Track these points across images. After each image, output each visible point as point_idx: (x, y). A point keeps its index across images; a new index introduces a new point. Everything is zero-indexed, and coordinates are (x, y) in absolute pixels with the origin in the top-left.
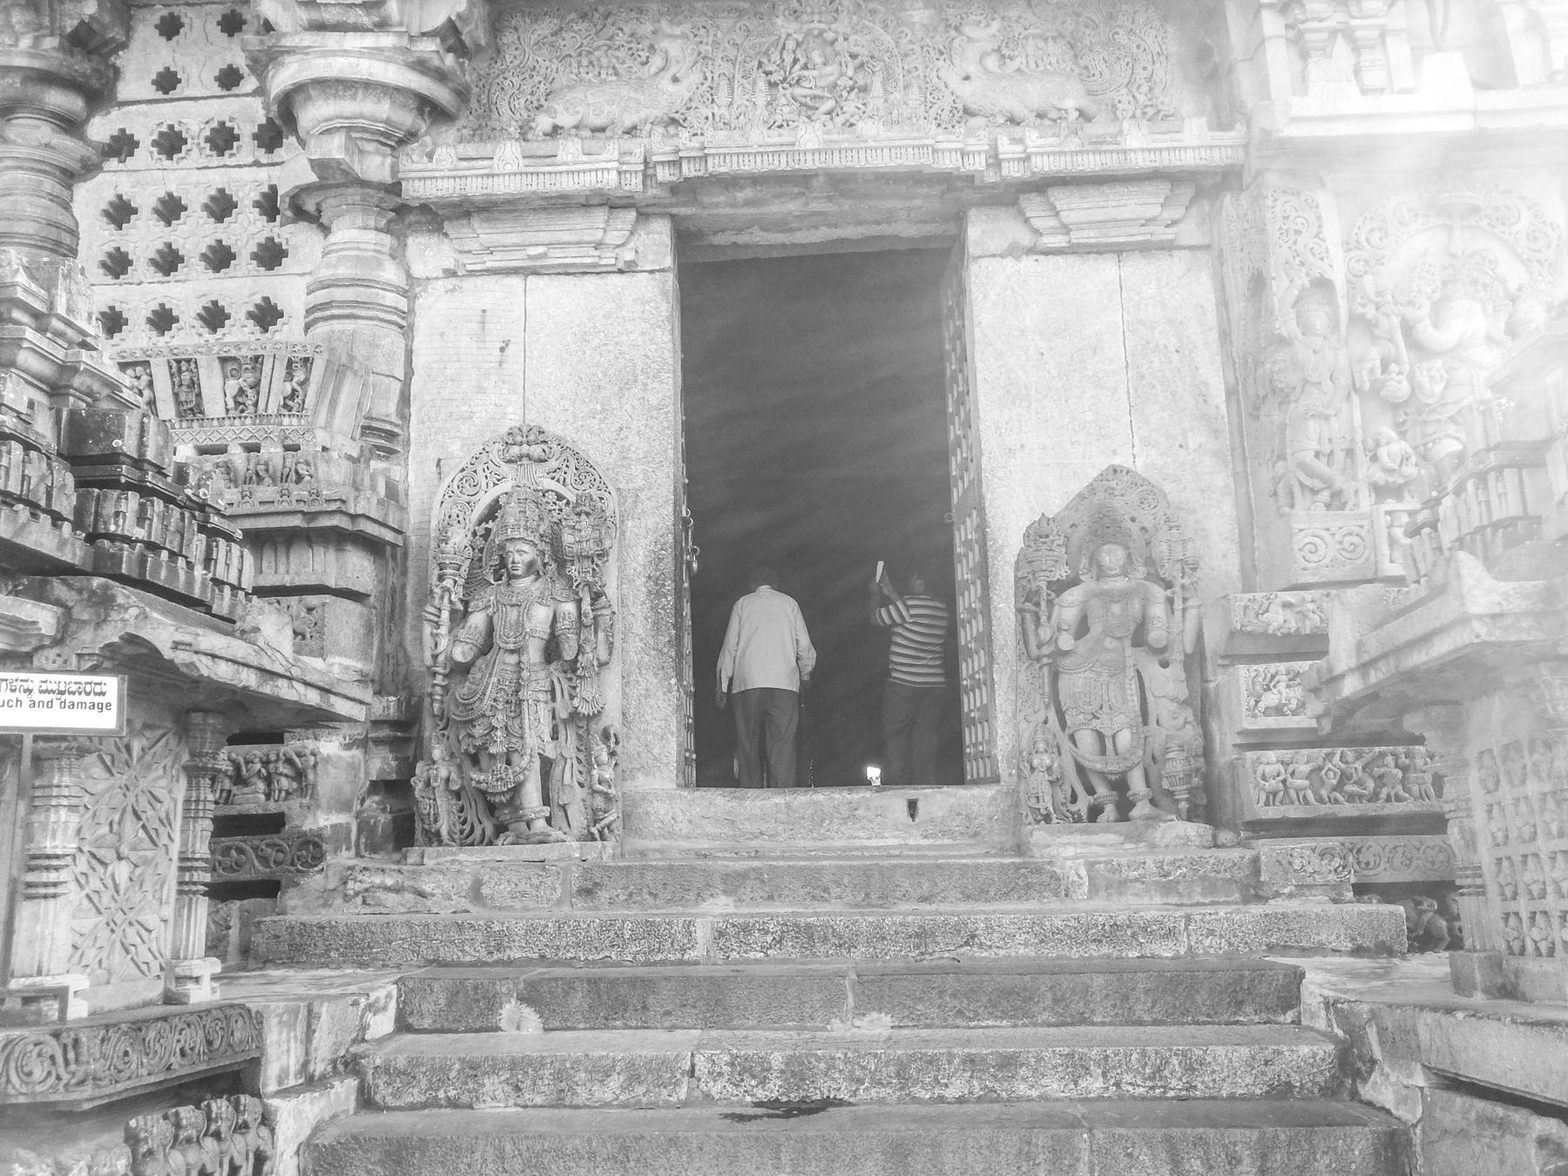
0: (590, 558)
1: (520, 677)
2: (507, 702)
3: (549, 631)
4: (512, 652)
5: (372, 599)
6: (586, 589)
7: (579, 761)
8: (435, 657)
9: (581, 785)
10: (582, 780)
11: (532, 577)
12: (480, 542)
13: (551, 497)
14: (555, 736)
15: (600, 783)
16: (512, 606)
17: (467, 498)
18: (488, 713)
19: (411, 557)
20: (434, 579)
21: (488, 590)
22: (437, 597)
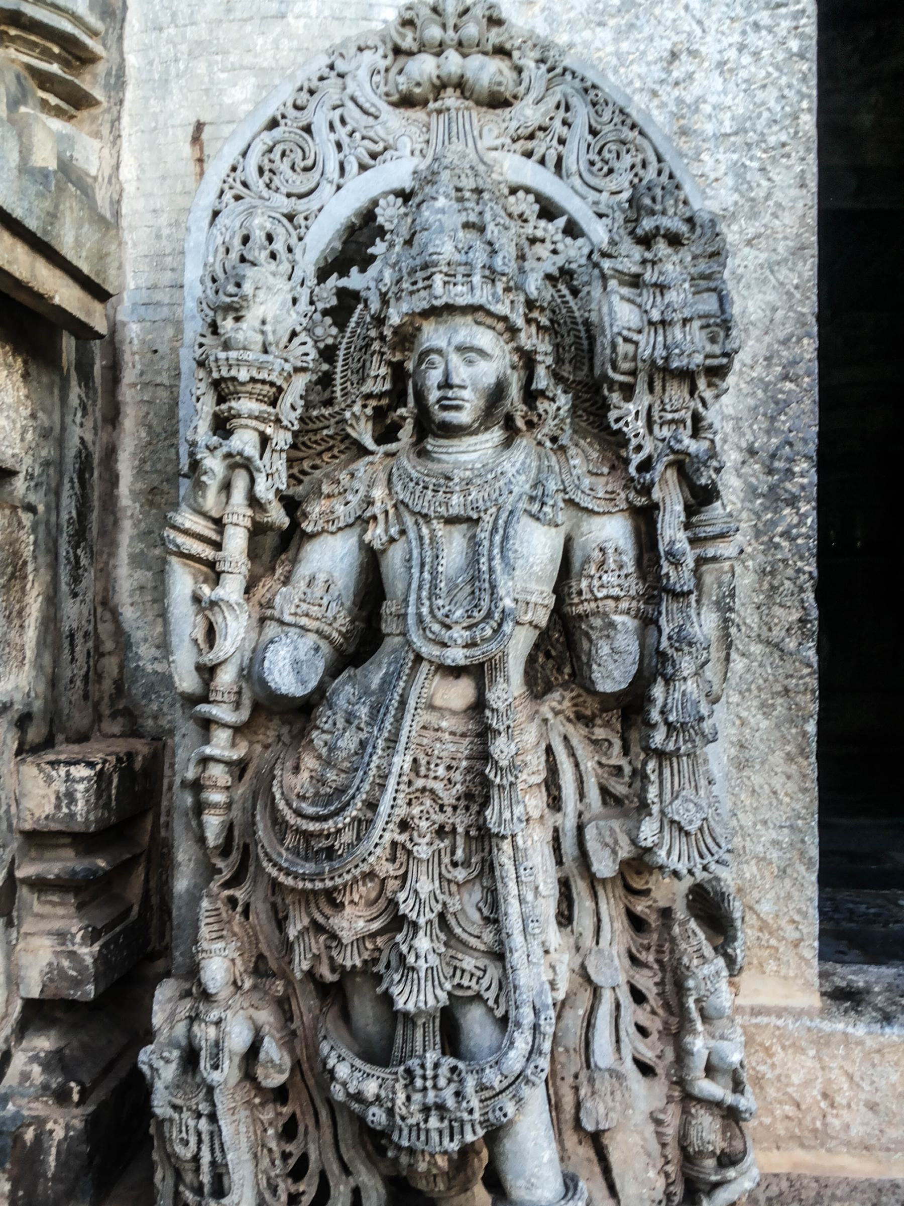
0: (687, 376)
1: (483, 756)
2: (441, 832)
3: (551, 601)
4: (456, 672)
5: (20, 485)
6: (672, 475)
7: (638, 997)
8: (208, 672)
9: (646, 1069)
10: (648, 1055)
11: (496, 435)
12: (327, 331)
13: (526, 205)
14: (565, 918)
15: (710, 1070)
16: (451, 521)
17: (287, 205)
18: (386, 869)
19: (129, 376)
20: (203, 432)
21: (361, 465)
22: (213, 484)
